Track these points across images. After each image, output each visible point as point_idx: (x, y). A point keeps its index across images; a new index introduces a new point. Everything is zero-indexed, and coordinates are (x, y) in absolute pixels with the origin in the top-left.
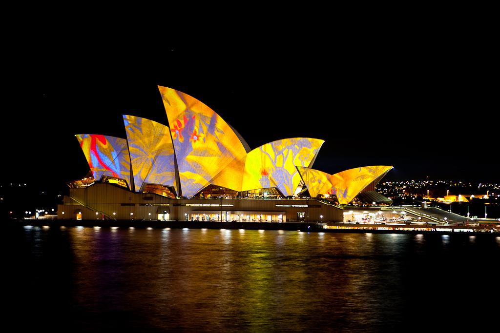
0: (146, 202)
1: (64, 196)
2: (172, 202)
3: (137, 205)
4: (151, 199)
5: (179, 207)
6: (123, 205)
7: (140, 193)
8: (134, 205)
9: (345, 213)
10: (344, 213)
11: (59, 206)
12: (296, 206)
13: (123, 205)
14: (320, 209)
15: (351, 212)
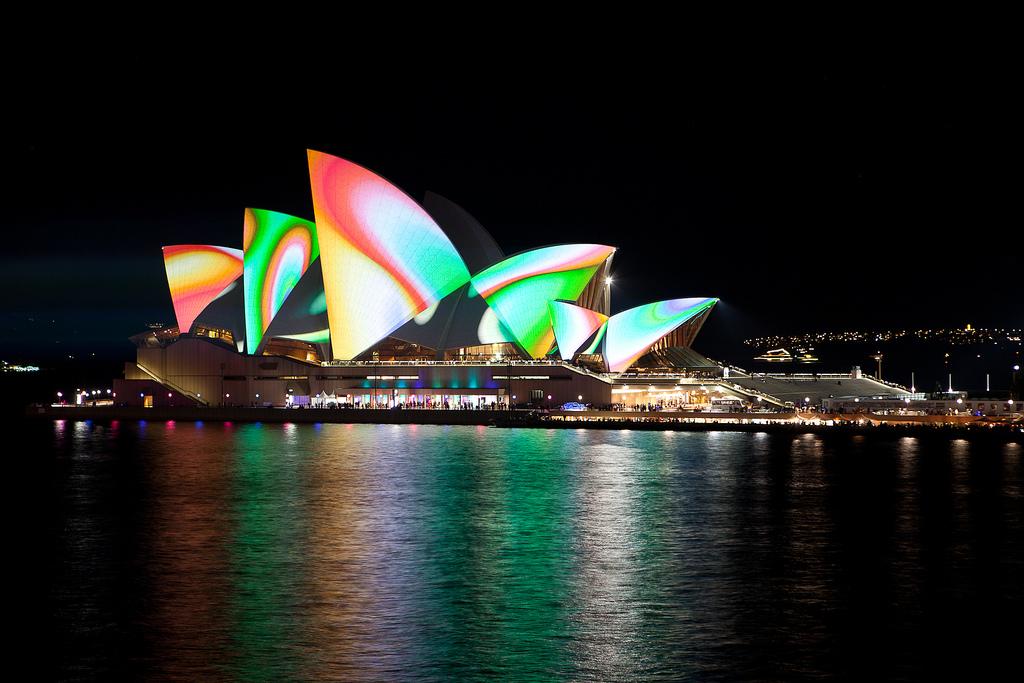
0: (266, 373)
1: (127, 364)
2: (314, 372)
3: (251, 380)
4: (274, 366)
5: (326, 382)
6: (226, 378)
7: (258, 354)
8: (244, 379)
9: (614, 391)
10: (614, 391)
11: (115, 381)
12: (527, 378)
13: (226, 378)
14: (570, 381)
15: (625, 389)
